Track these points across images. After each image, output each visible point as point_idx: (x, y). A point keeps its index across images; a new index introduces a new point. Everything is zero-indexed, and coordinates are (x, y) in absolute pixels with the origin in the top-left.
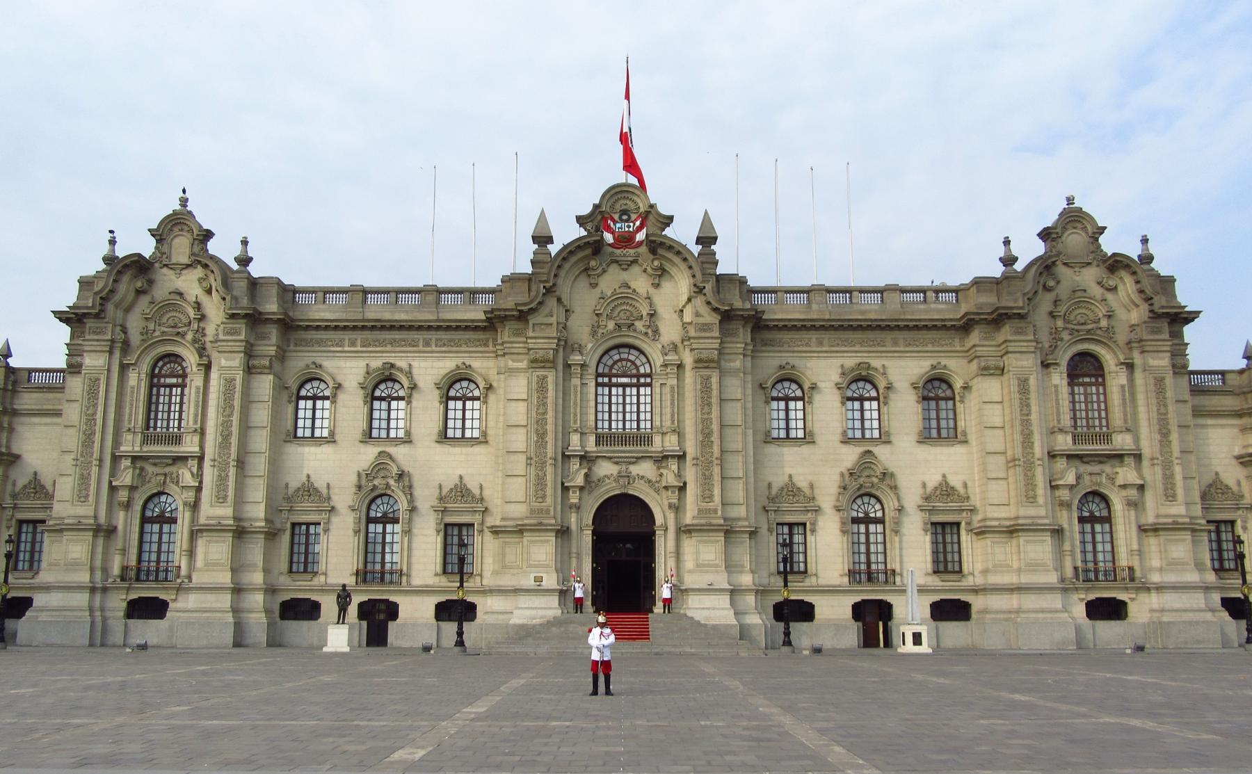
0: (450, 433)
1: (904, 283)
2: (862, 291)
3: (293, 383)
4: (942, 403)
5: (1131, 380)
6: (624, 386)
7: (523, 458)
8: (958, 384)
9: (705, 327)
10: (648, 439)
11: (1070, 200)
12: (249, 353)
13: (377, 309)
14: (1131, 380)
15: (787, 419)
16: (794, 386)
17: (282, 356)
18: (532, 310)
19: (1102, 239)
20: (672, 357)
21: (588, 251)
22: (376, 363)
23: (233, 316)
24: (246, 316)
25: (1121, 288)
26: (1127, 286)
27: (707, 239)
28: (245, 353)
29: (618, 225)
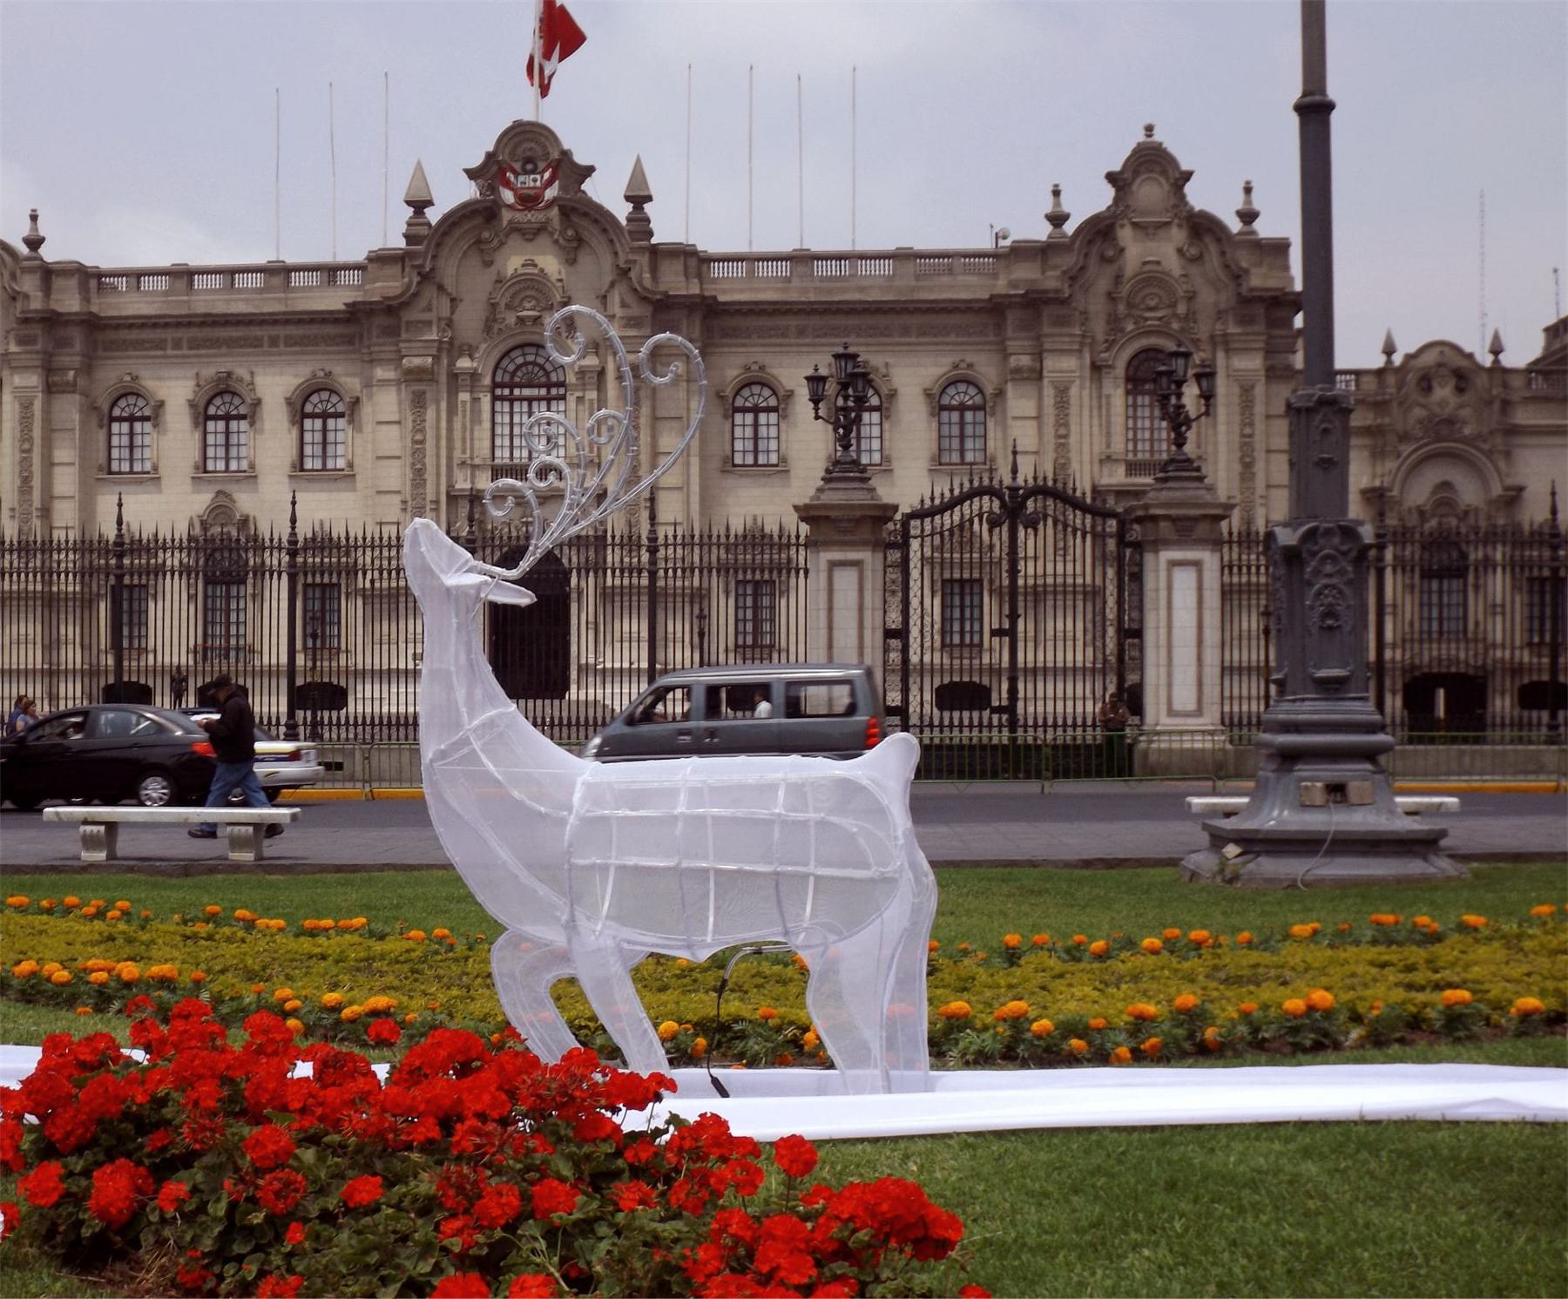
0: (308, 464)
1: (919, 246)
2: (863, 257)
4: (969, 416)
6: (530, 400)
7: (396, 499)
8: (989, 390)
11: (1149, 129)
12: (48, 369)
13: (208, 298)
15: (756, 438)
16: (767, 392)
17: (88, 368)
18: (405, 305)
19: (1189, 189)
21: (479, 220)
22: (209, 372)
23: (25, 321)
24: (43, 320)
25: (1207, 257)
28: (43, 367)
29: (521, 178)
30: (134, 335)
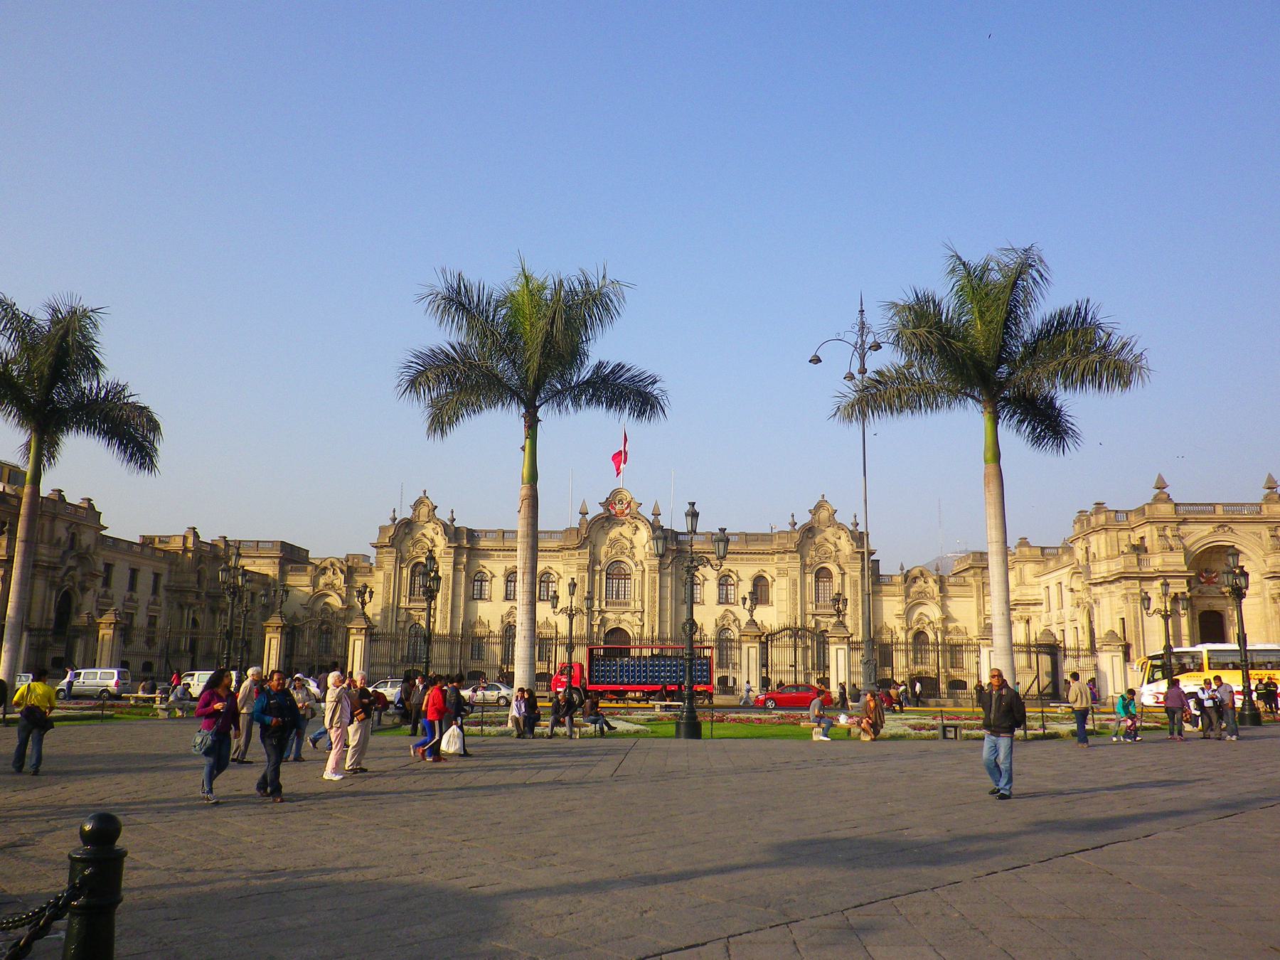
3: (472, 574)
5: (843, 580)
8: (770, 579)
10: (627, 604)
12: (456, 564)
14: (843, 580)
20: (640, 567)
22: (510, 566)
26: (844, 536)
27: (656, 514)
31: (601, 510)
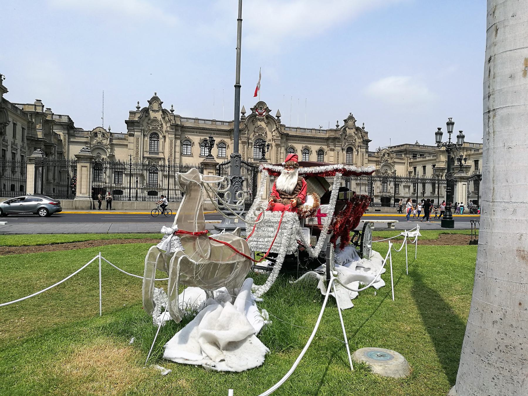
9: (277, 137)
13: (201, 125)
30: (189, 130)
31: (251, 112)
